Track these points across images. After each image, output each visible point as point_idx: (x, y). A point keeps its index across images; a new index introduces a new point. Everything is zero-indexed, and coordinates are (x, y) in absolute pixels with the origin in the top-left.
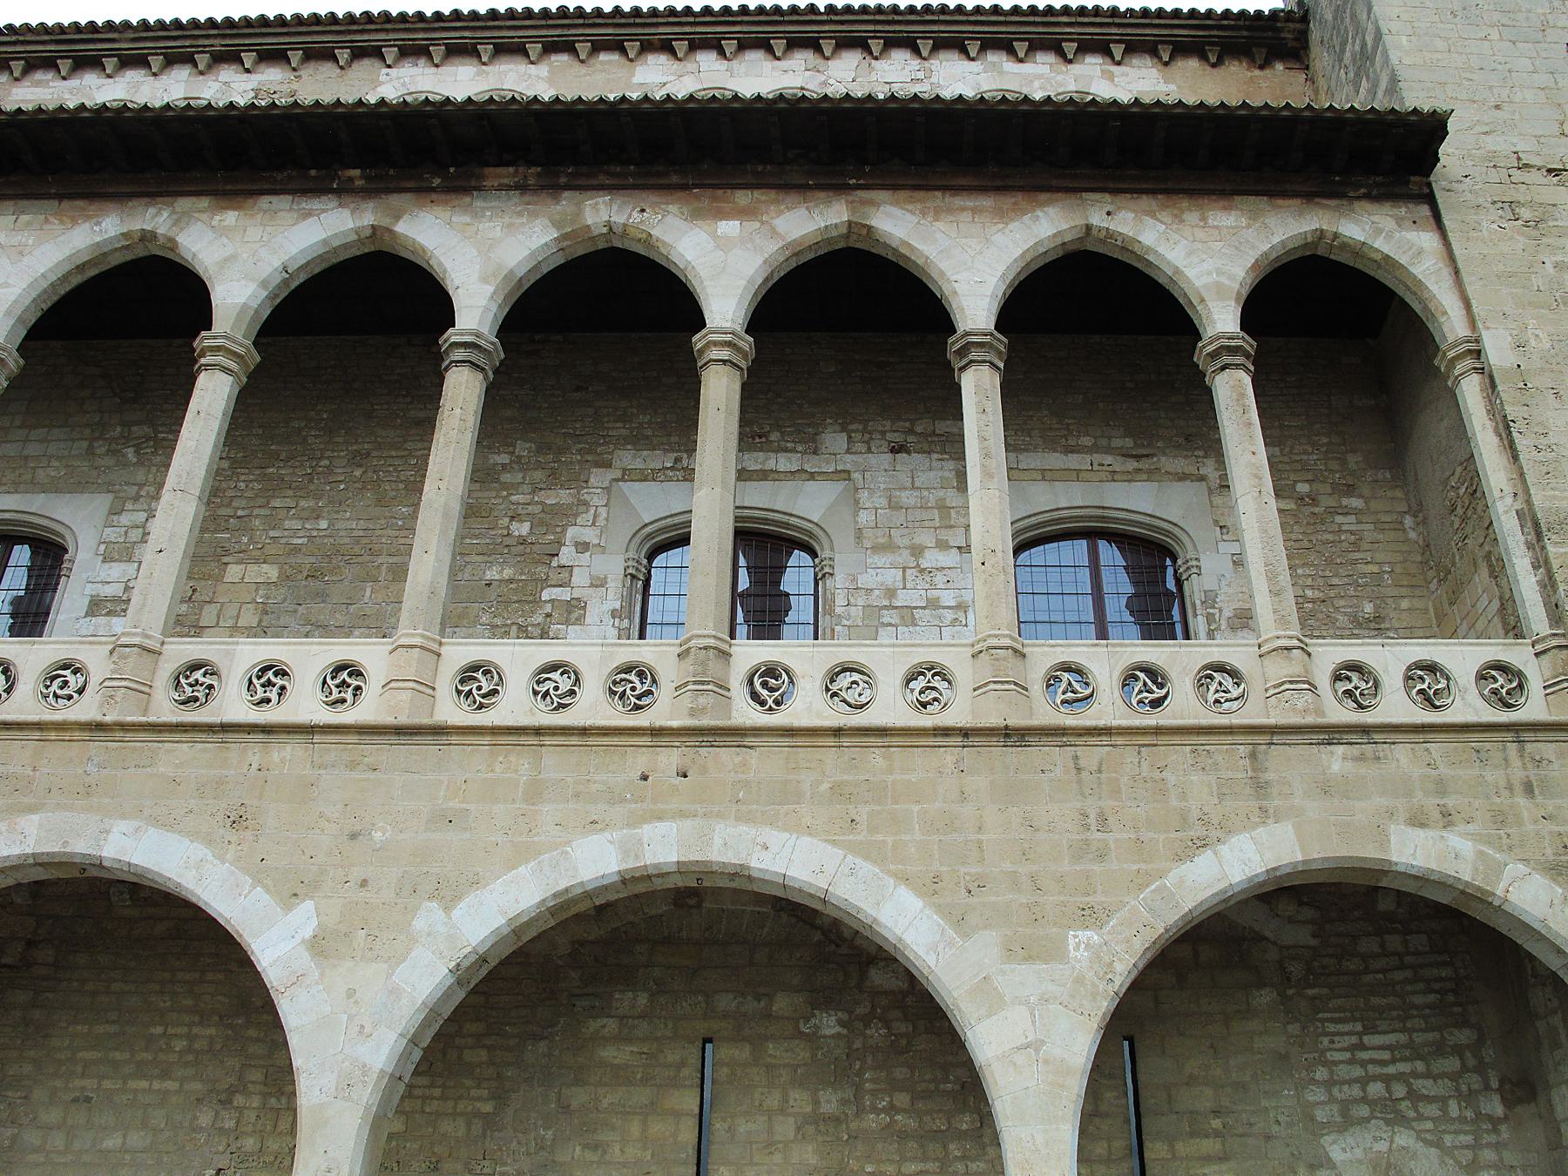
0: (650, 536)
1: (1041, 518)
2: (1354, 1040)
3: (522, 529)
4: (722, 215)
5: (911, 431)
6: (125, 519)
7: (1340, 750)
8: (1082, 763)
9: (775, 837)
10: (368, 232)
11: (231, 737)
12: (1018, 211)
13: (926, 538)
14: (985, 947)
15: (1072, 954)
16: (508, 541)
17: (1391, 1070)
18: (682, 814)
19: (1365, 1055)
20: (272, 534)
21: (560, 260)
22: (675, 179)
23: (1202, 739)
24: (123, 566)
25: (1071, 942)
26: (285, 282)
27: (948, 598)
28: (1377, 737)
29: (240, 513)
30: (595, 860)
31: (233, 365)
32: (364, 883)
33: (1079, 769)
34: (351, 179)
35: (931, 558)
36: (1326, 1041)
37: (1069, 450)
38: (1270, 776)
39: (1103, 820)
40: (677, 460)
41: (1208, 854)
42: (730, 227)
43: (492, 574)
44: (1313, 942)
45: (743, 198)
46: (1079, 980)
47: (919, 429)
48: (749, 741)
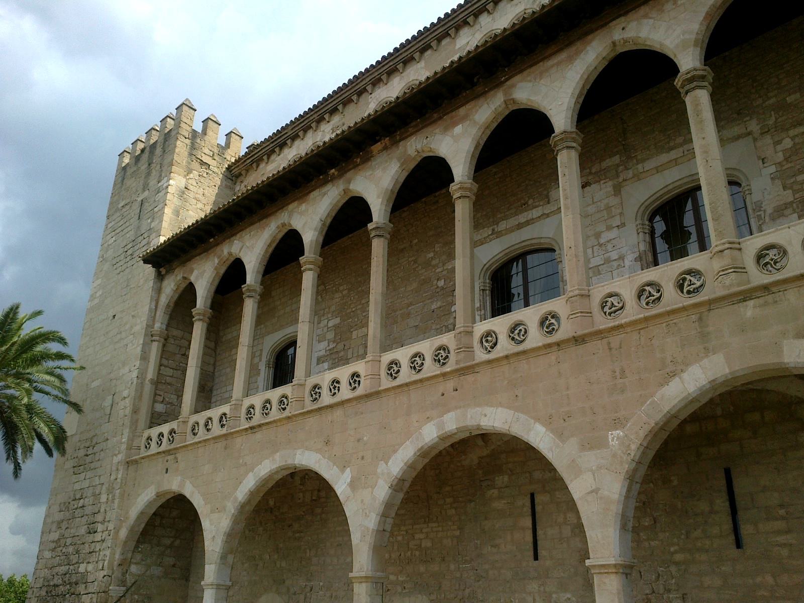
0: (487, 269)
3: (441, 283)
4: (455, 124)
6: (322, 325)
7: (751, 303)
8: (612, 345)
9: (489, 410)
12: (578, 53)
13: (601, 227)
14: (572, 446)
15: (611, 443)
18: (456, 408)
20: (364, 314)
21: (405, 174)
22: (435, 116)
23: (672, 317)
24: (324, 343)
25: (610, 437)
28: (774, 289)
29: (353, 310)
31: (311, 266)
32: (363, 458)
33: (610, 349)
35: (605, 237)
37: (671, 149)
38: (711, 329)
40: (493, 230)
41: (677, 379)
42: (458, 129)
45: (462, 111)
46: (614, 455)
48: (477, 369)
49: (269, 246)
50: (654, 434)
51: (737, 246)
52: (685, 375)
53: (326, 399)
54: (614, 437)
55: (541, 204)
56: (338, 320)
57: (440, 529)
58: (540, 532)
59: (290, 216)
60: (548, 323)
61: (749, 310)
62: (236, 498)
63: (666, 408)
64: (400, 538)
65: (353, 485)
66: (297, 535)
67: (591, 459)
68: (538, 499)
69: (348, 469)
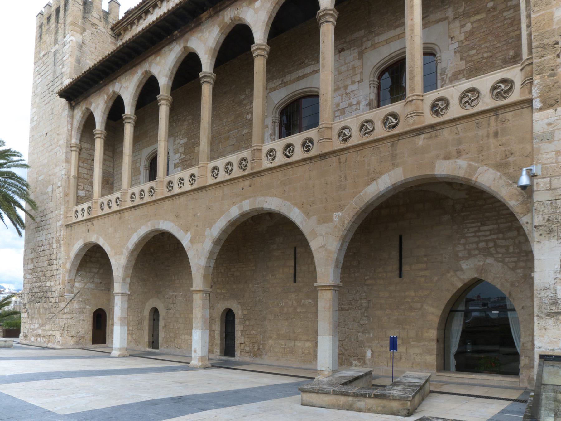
0: (278, 108)
1: (385, 60)
2: (477, 229)
5: (345, 42)
7: (423, 136)
8: (341, 160)
9: (268, 199)
10: (183, 49)
11: (174, 198)
13: (349, 82)
15: (334, 219)
16: (247, 121)
17: (489, 238)
18: (250, 197)
19: (480, 234)
23: (377, 144)
25: (334, 216)
26: (172, 73)
27: (354, 102)
28: (437, 128)
30: (234, 212)
32: (197, 226)
33: (340, 163)
34: (177, 34)
35: (351, 88)
36: (466, 230)
38: (398, 152)
39: (346, 177)
40: (283, 80)
41: (375, 182)
43: (244, 132)
44: (467, 196)
46: (336, 227)
47: (347, 40)
48: (263, 174)
49: (138, 87)
50: (359, 215)
51: (421, 98)
52: (380, 181)
53: (176, 190)
54: (337, 215)
55: (313, 63)
56: (186, 140)
57: (245, 266)
58: (298, 268)
59: (150, 66)
60: (307, 145)
61: (421, 141)
62: (128, 247)
63: (366, 201)
64: (222, 271)
65: (192, 241)
66: (167, 268)
67: (323, 229)
68: (298, 250)
69: (189, 233)
